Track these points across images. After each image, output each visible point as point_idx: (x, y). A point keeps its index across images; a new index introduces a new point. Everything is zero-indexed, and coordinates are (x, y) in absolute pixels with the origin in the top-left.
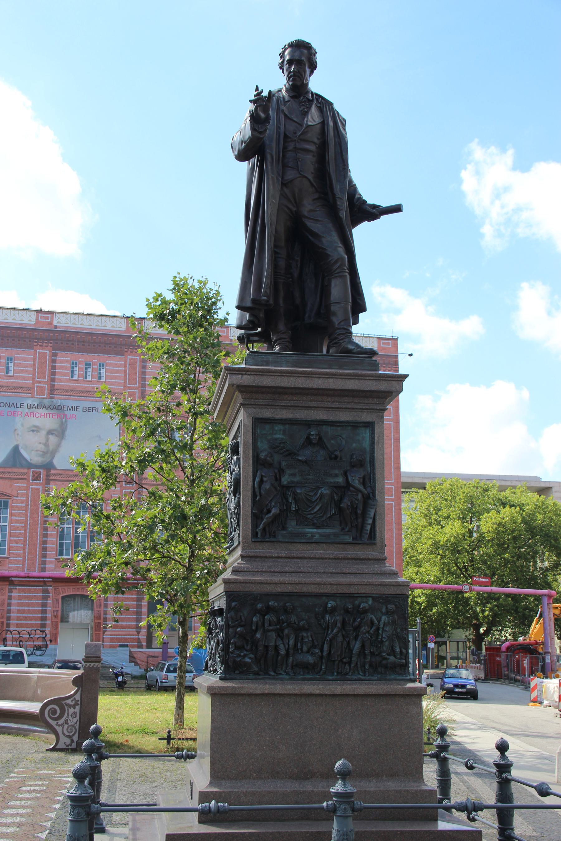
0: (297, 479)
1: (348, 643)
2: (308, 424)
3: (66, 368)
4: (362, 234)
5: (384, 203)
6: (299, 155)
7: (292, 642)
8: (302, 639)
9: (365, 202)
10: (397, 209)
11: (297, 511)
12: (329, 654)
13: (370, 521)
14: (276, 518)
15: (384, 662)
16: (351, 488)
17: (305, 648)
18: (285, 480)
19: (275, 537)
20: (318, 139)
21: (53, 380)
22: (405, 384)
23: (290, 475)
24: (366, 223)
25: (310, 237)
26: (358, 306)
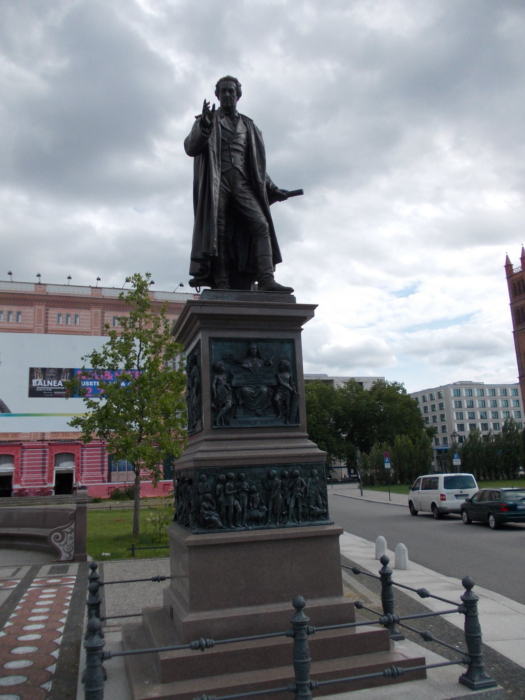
0: (243, 381)
1: (286, 501)
2: (248, 341)
3: (54, 318)
4: (278, 210)
5: (290, 189)
6: (232, 154)
7: (246, 503)
8: (253, 499)
9: (277, 188)
10: (300, 192)
11: (243, 405)
12: (273, 510)
13: (296, 410)
14: (229, 411)
15: (312, 512)
16: (281, 387)
17: (256, 506)
18: (234, 383)
19: (228, 424)
20: (245, 143)
21: (47, 325)
22: (316, 311)
23: (237, 378)
24: (278, 203)
25: (242, 211)
26: (277, 259)
